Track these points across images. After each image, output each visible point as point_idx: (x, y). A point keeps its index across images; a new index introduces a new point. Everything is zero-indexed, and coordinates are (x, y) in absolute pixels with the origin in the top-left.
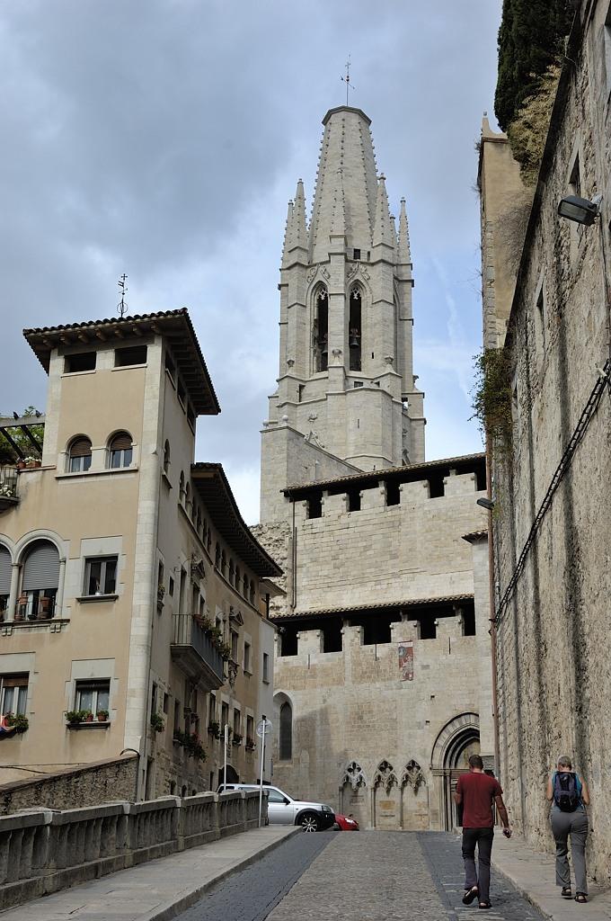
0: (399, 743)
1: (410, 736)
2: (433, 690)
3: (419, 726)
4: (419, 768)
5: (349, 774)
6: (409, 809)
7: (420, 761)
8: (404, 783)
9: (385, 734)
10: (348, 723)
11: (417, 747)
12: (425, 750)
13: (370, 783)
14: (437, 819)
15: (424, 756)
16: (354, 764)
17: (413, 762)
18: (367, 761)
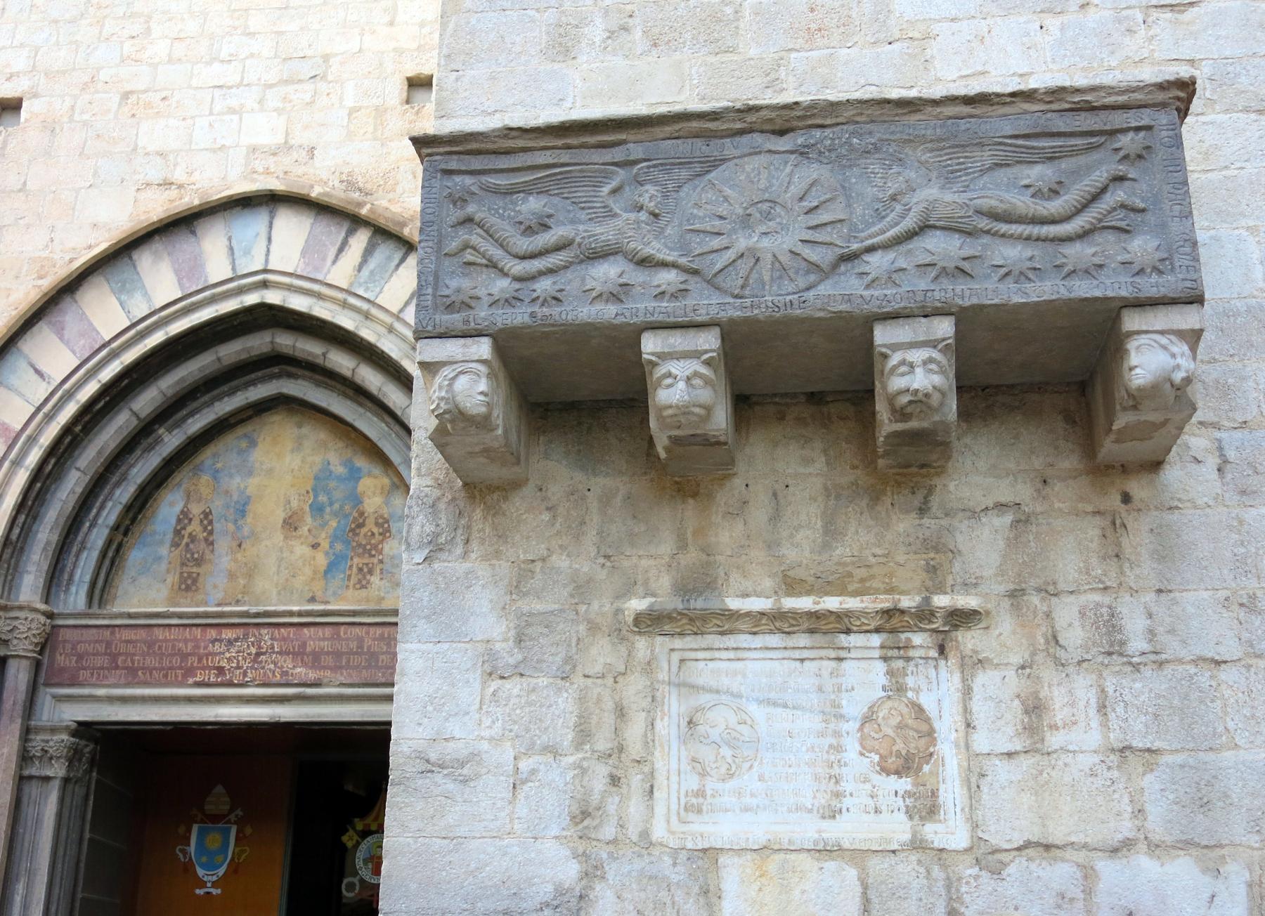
2: (20, 62)
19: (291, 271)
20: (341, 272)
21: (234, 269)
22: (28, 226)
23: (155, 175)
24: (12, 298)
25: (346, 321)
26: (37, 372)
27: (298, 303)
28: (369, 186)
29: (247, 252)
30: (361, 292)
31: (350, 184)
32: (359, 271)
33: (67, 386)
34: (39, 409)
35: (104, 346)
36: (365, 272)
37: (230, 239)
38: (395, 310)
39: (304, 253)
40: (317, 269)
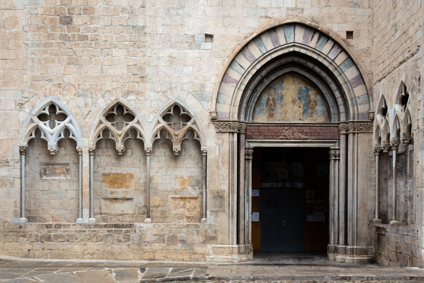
0: (149, 71)
1: (172, 59)
3: (192, 42)
4: (187, 118)
5: (41, 124)
6: (161, 188)
7: (191, 105)
8: (156, 143)
9: (119, 54)
10: (39, 28)
11: (186, 80)
12: (203, 86)
13: (86, 142)
14: (221, 206)
15: (200, 96)
16: (52, 107)
17: (177, 108)
18: (81, 101)
19: (300, 43)
20: (313, 43)
21: (286, 41)
22: (232, 27)
23: (263, 14)
24: (231, 47)
25: (315, 56)
26: (241, 66)
27: (303, 51)
28: (317, 21)
29: (289, 37)
30: (318, 49)
31: (313, 20)
32: (317, 43)
33: (249, 70)
34: (242, 76)
35: (257, 60)
36: (319, 44)
37: (285, 33)
38: (326, 54)
39: (303, 38)
40: (307, 43)
